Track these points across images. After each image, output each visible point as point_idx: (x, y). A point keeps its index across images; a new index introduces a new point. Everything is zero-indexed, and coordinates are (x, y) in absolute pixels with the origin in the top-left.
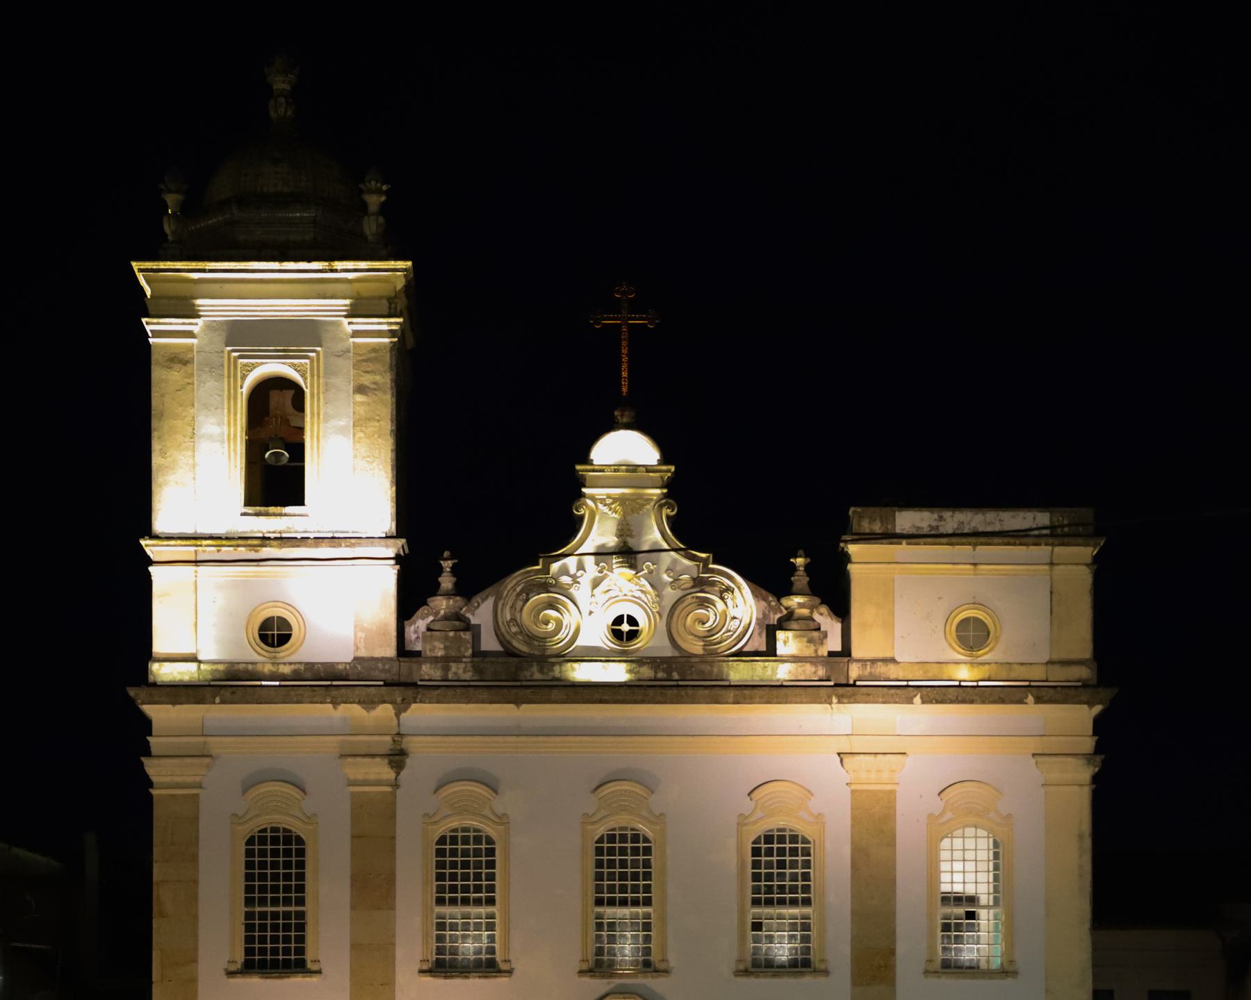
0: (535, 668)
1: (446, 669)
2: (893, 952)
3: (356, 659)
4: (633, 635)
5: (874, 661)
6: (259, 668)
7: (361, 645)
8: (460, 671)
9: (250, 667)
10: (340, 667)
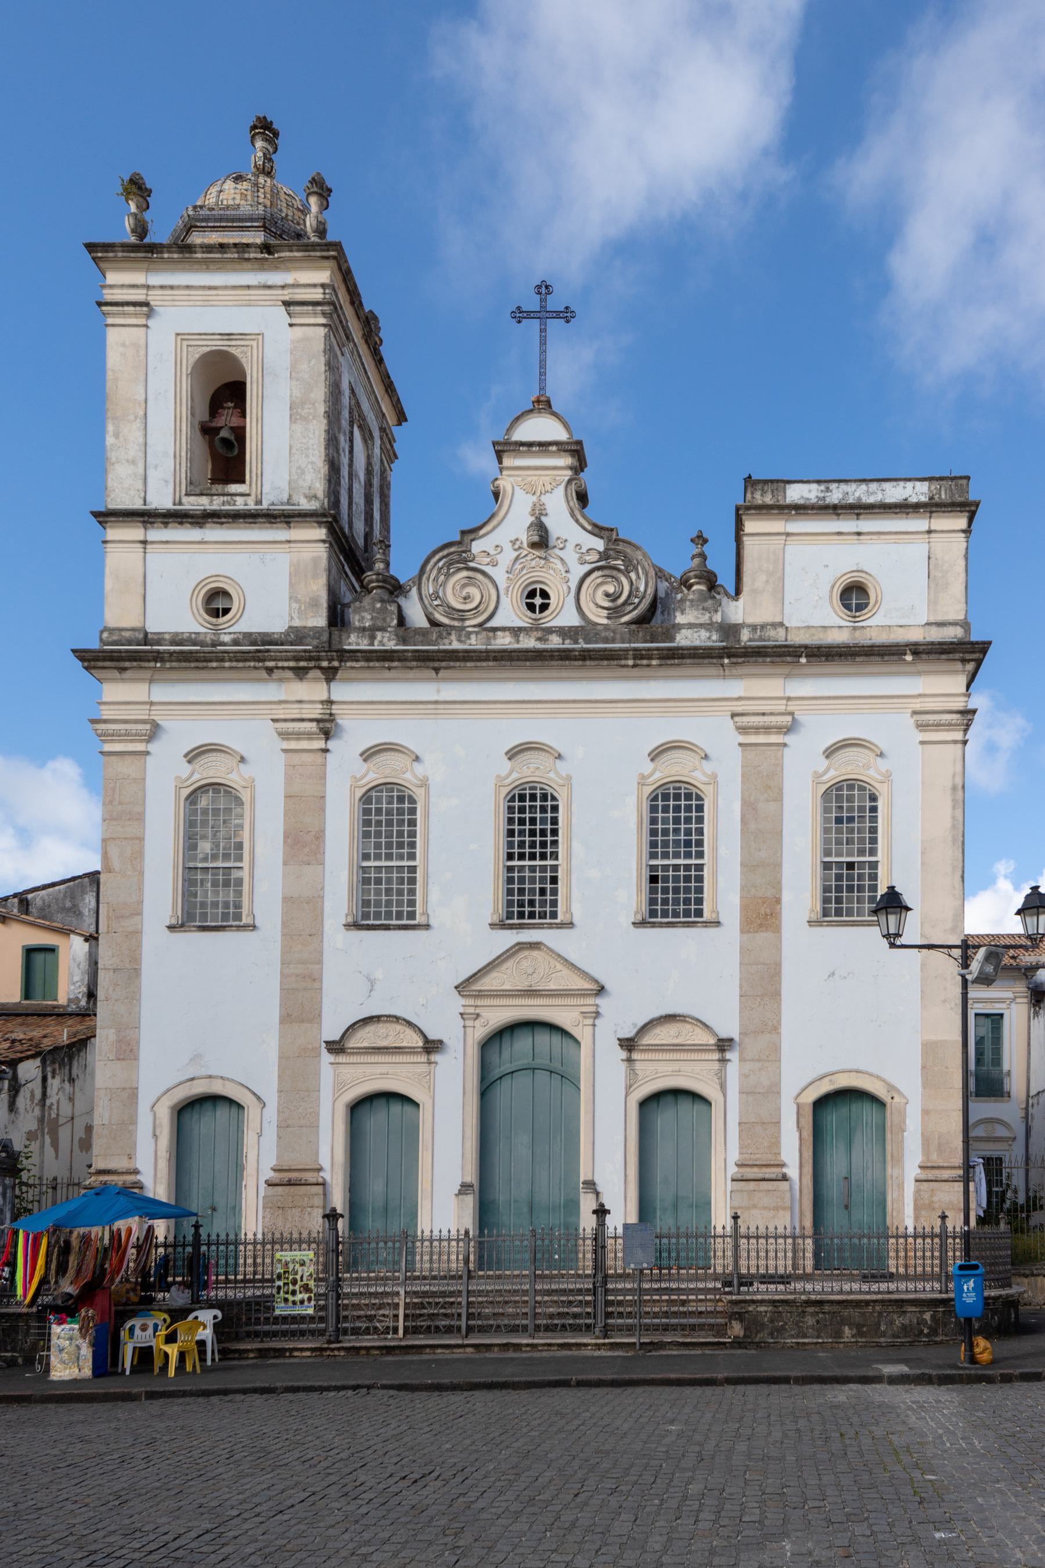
1: (373, 638)
2: (778, 901)
3: (290, 627)
4: (544, 607)
5: (763, 627)
6: (202, 637)
7: (295, 616)
9: (193, 636)
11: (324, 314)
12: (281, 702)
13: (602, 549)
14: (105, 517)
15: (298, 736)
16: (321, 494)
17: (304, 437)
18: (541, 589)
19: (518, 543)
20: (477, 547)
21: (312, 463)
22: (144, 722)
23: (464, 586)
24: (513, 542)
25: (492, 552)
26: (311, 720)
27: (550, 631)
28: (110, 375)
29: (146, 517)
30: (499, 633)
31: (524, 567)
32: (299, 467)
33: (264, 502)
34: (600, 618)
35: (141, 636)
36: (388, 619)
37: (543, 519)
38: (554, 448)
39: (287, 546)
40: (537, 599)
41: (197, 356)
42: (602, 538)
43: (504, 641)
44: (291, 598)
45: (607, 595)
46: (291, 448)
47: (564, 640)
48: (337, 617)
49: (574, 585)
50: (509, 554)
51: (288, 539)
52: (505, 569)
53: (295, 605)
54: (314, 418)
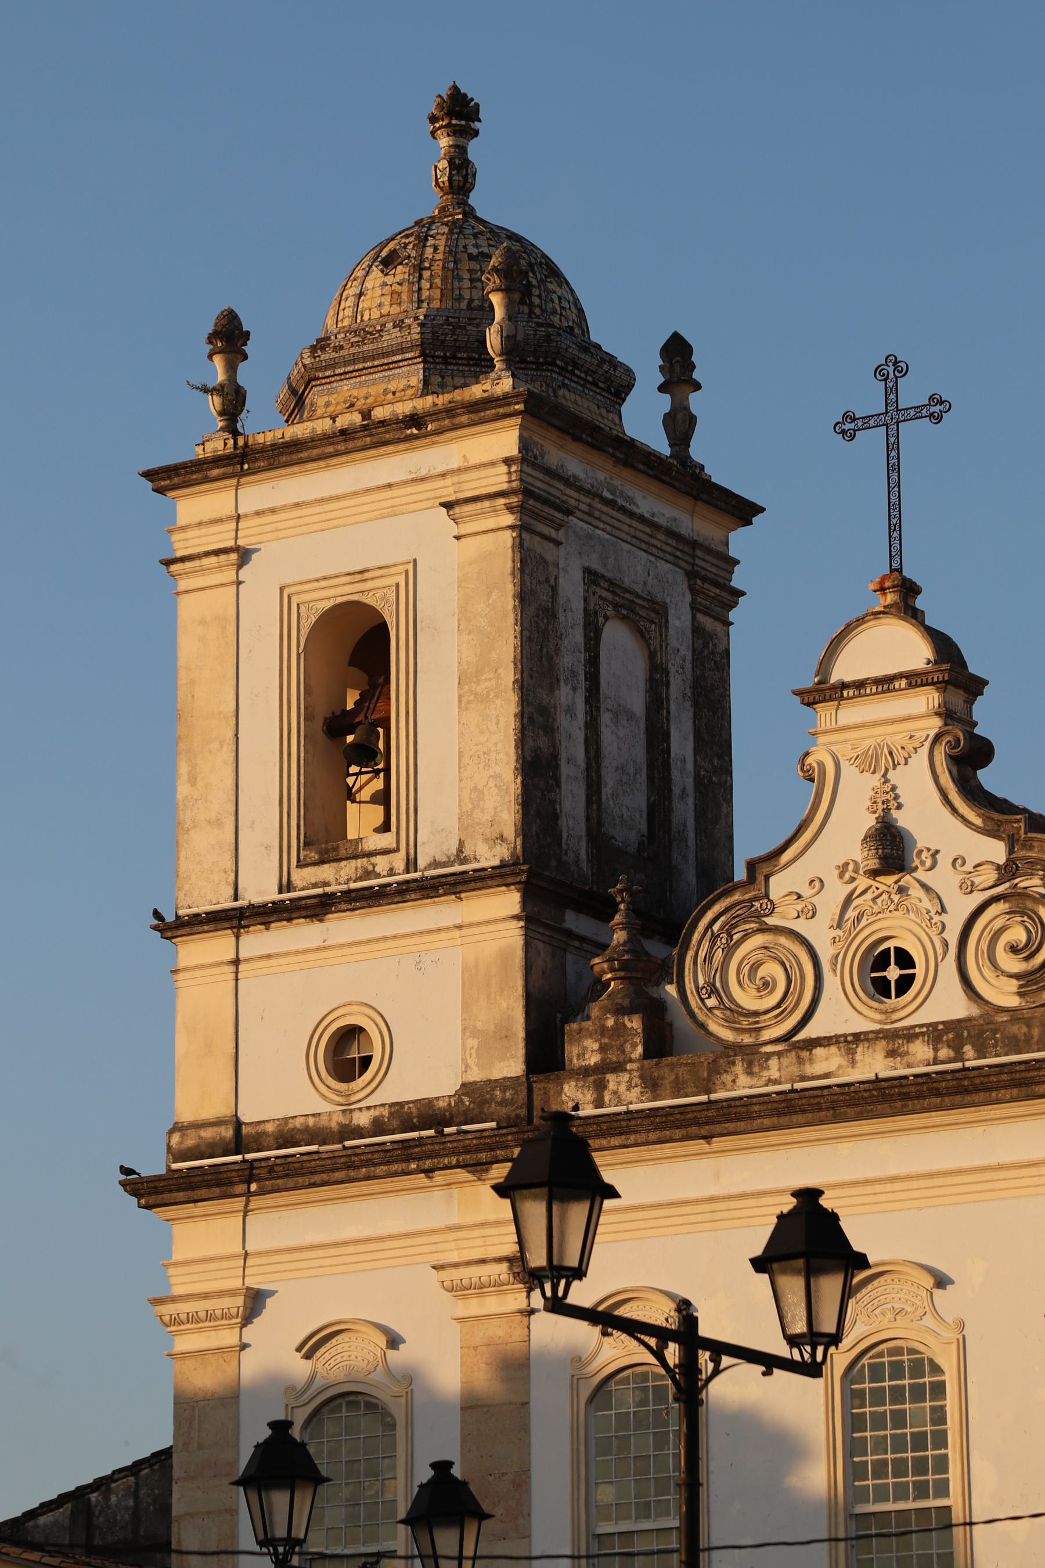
0: (739, 1068)
1: (600, 1086)
3: (463, 1085)
4: (905, 984)
6: (324, 1121)
7: (472, 1062)
8: (622, 1088)
9: (311, 1121)
10: (442, 1104)
11: (509, 508)
12: (450, 1229)
13: (1001, 859)
14: (174, 927)
15: (481, 1288)
16: (510, 832)
17: (482, 732)
18: (897, 949)
19: (851, 867)
20: (779, 885)
21: (497, 776)
22: (232, 1293)
23: (755, 967)
24: (843, 869)
25: (806, 891)
26: (499, 1260)
27: (909, 1035)
28: (183, 677)
29: (237, 919)
30: (819, 1051)
31: (859, 919)
32: (475, 788)
33: (422, 863)
34: (1003, 994)
35: (228, 1133)
36: (628, 1047)
37: (895, 814)
38: (903, 683)
39: (457, 933)
40: (887, 972)
41: (314, 620)
42: (999, 838)
43: (829, 1067)
44: (464, 1029)
45: (1014, 949)
46: (460, 752)
47: (936, 1050)
48: (545, 1054)
49: (953, 936)
50: (836, 891)
51: (459, 921)
52: (828, 924)
53: (473, 1042)
54: (496, 696)
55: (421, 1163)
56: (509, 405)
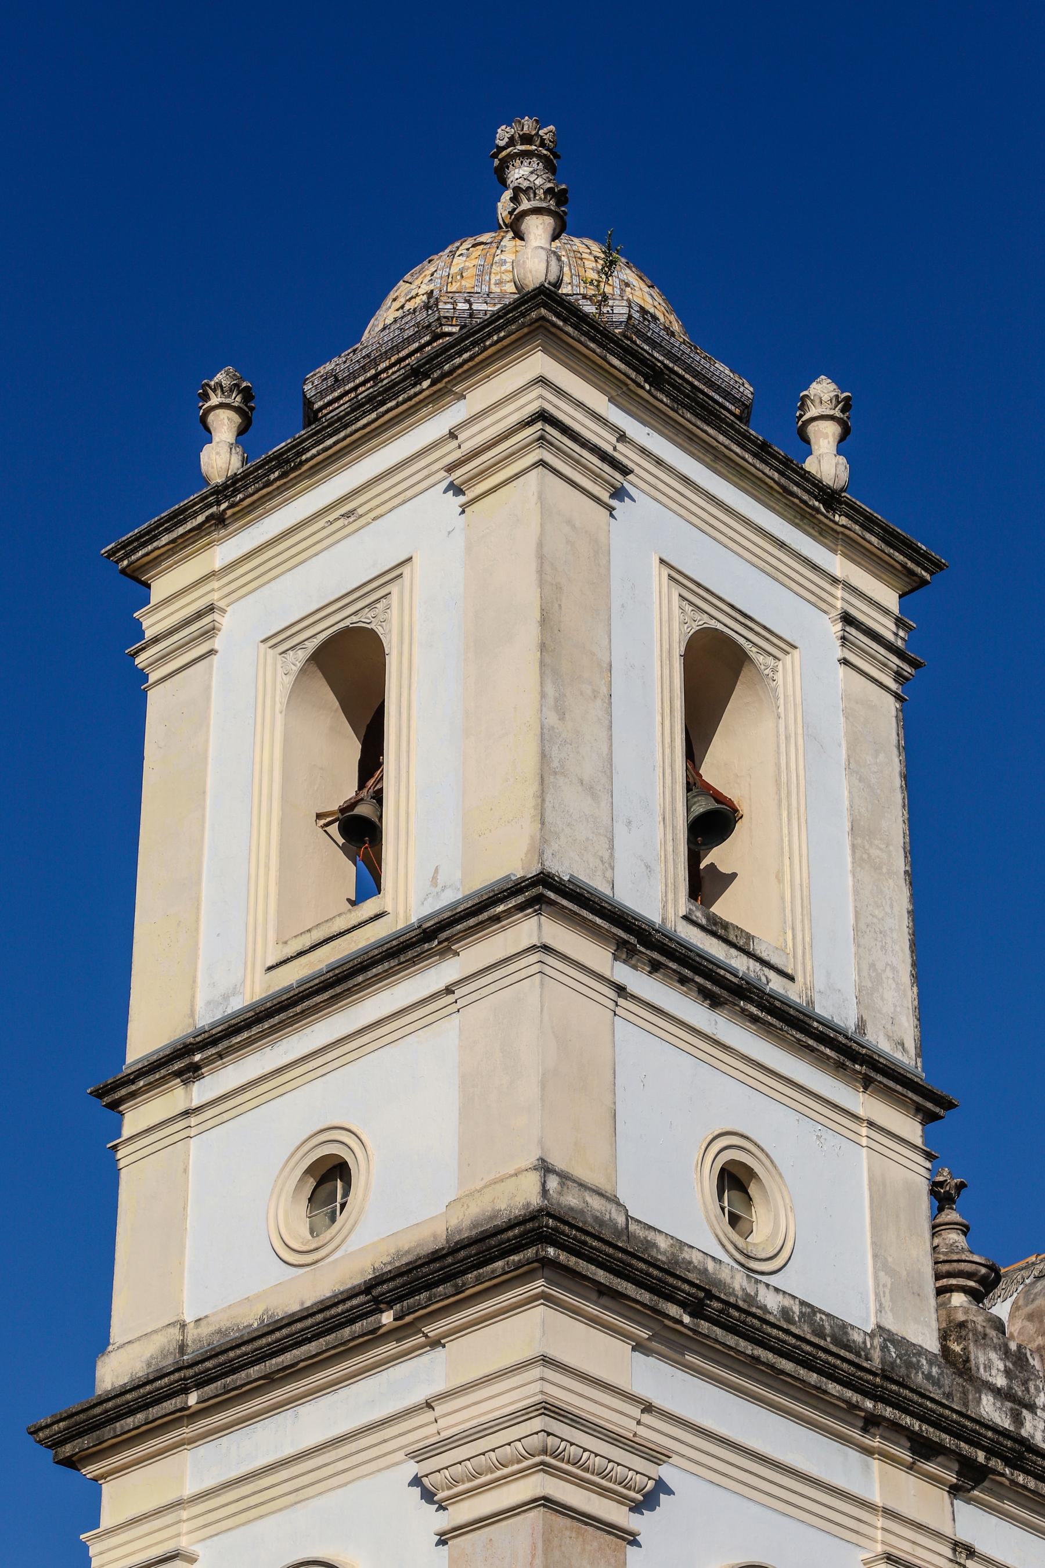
55: (880, 1405)
56: (918, 564)
